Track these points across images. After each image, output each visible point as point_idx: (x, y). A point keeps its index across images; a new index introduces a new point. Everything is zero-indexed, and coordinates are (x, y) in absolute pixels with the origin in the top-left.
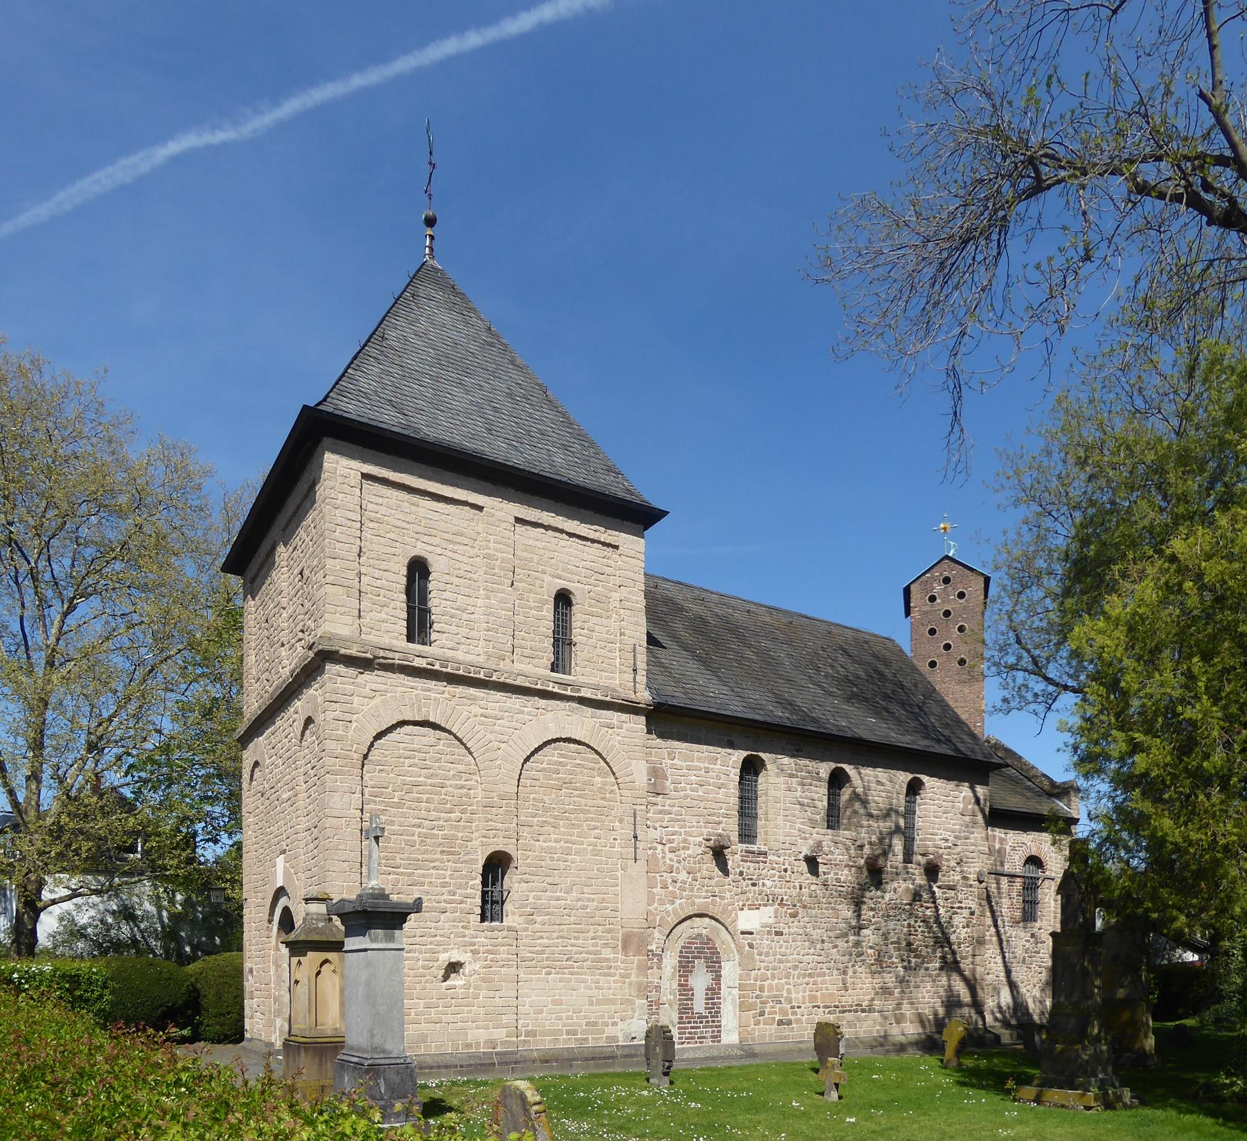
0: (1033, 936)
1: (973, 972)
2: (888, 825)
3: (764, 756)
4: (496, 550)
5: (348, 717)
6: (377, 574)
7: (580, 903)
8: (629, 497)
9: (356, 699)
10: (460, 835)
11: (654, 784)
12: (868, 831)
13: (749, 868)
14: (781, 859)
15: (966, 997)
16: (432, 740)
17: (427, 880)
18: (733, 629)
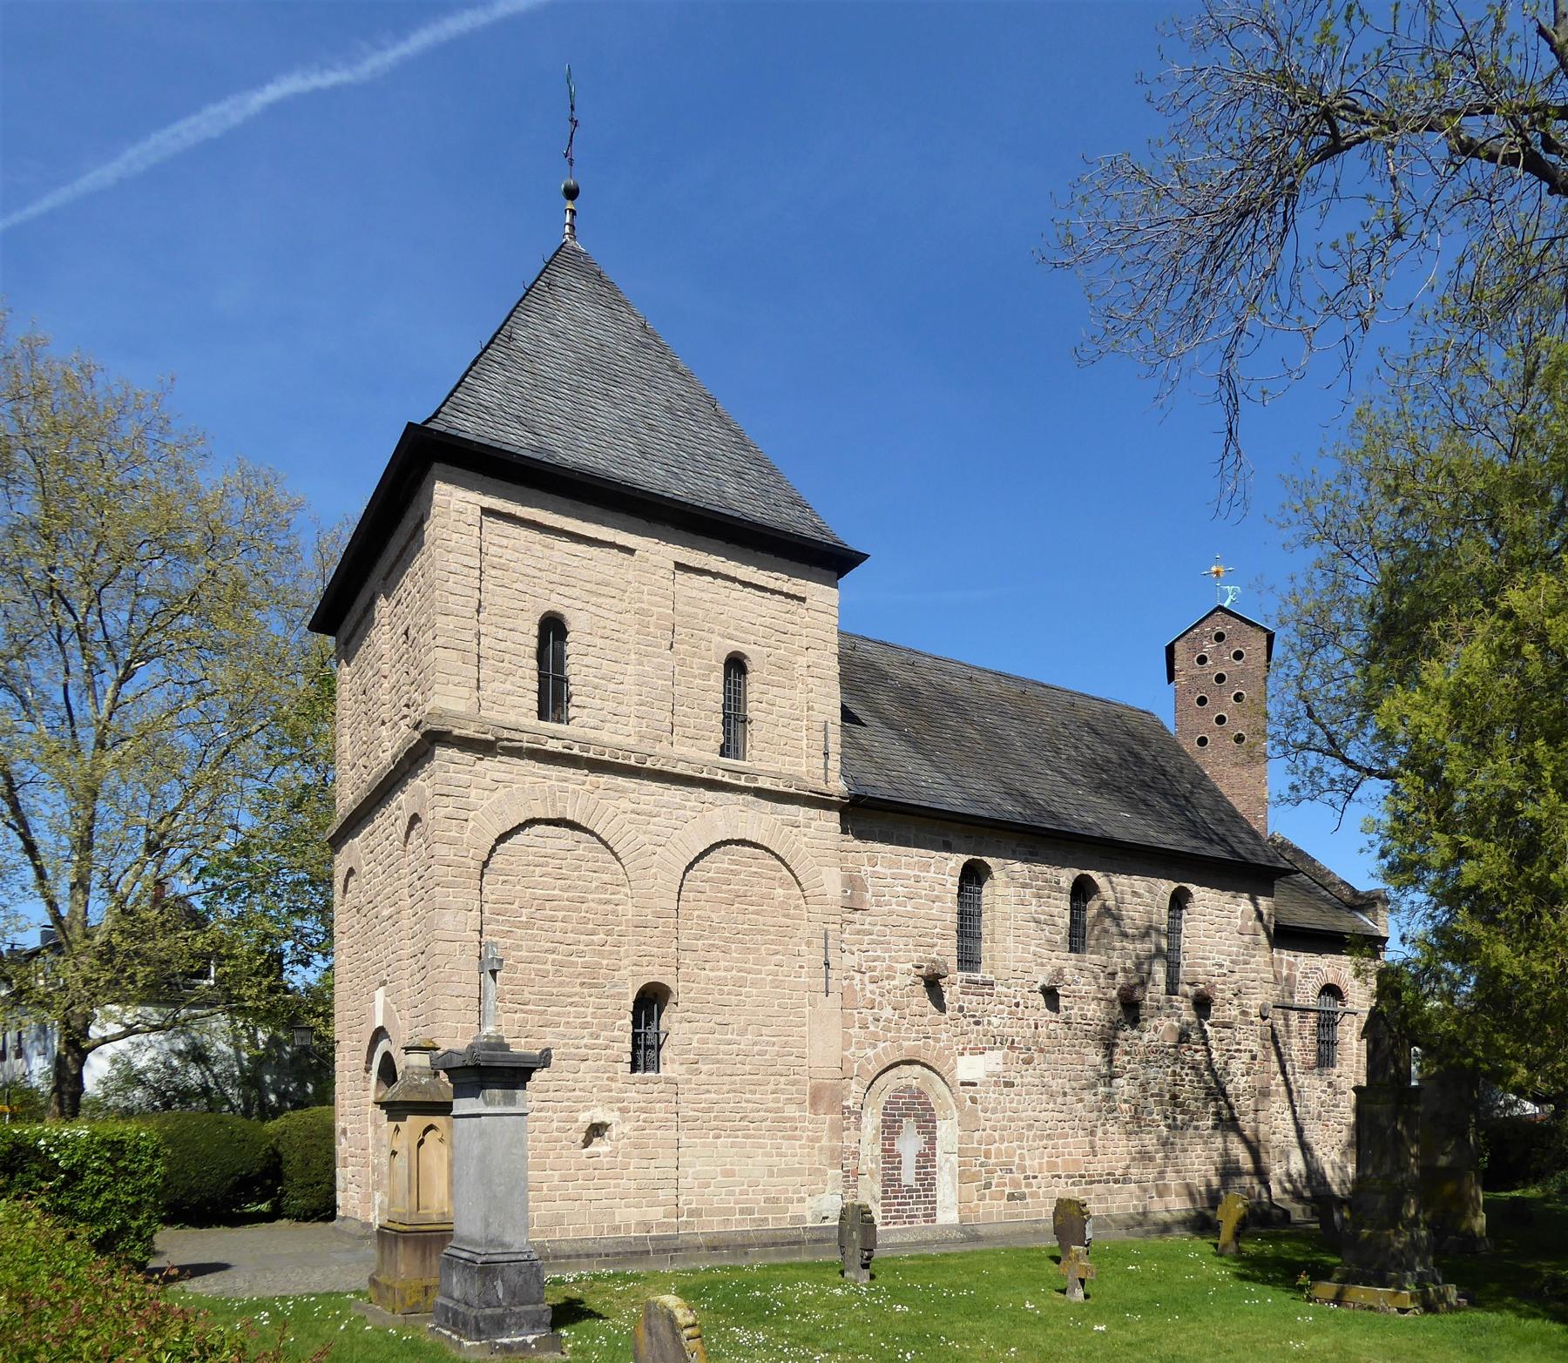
0: (1330, 1085)
1: (1256, 1131)
2: (1148, 946)
3: (988, 860)
4: (651, 604)
5: (463, 814)
6: (501, 634)
7: (757, 1048)
8: (818, 537)
9: (473, 792)
10: (605, 962)
11: (851, 897)
12: (1123, 956)
13: (970, 1002)
14: (1012, 991)
15: (1246, 1161)
16: (570, 843)
17: (563, 1020)
18: (952, 702)
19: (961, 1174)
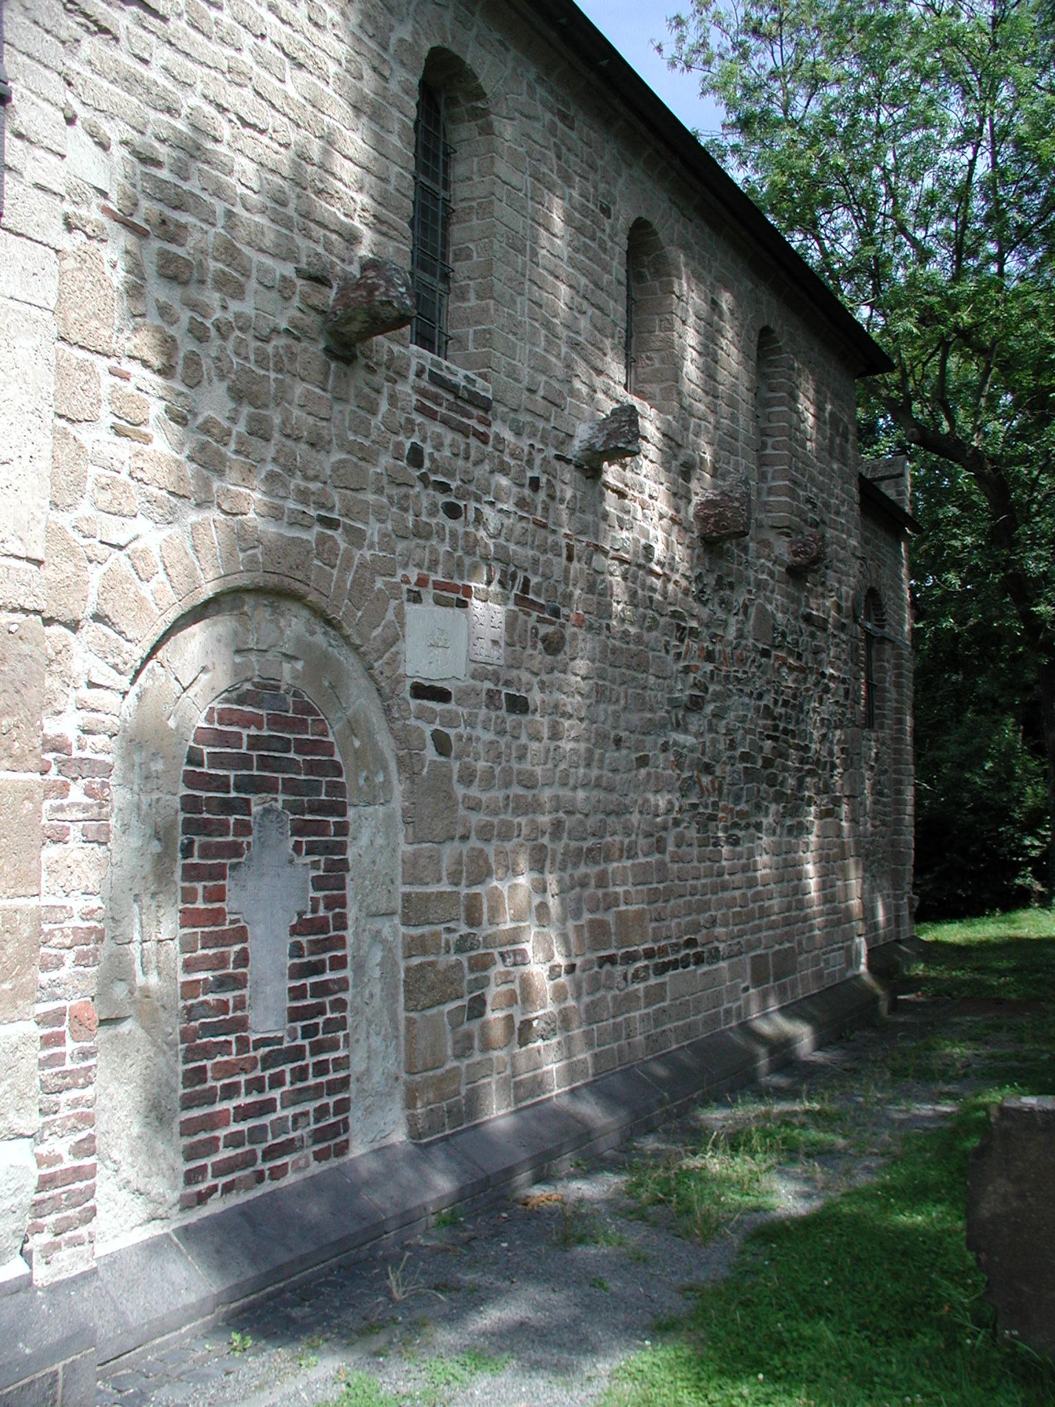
13: (439, 441)
14: (524, 443)
19: (415, 977)
